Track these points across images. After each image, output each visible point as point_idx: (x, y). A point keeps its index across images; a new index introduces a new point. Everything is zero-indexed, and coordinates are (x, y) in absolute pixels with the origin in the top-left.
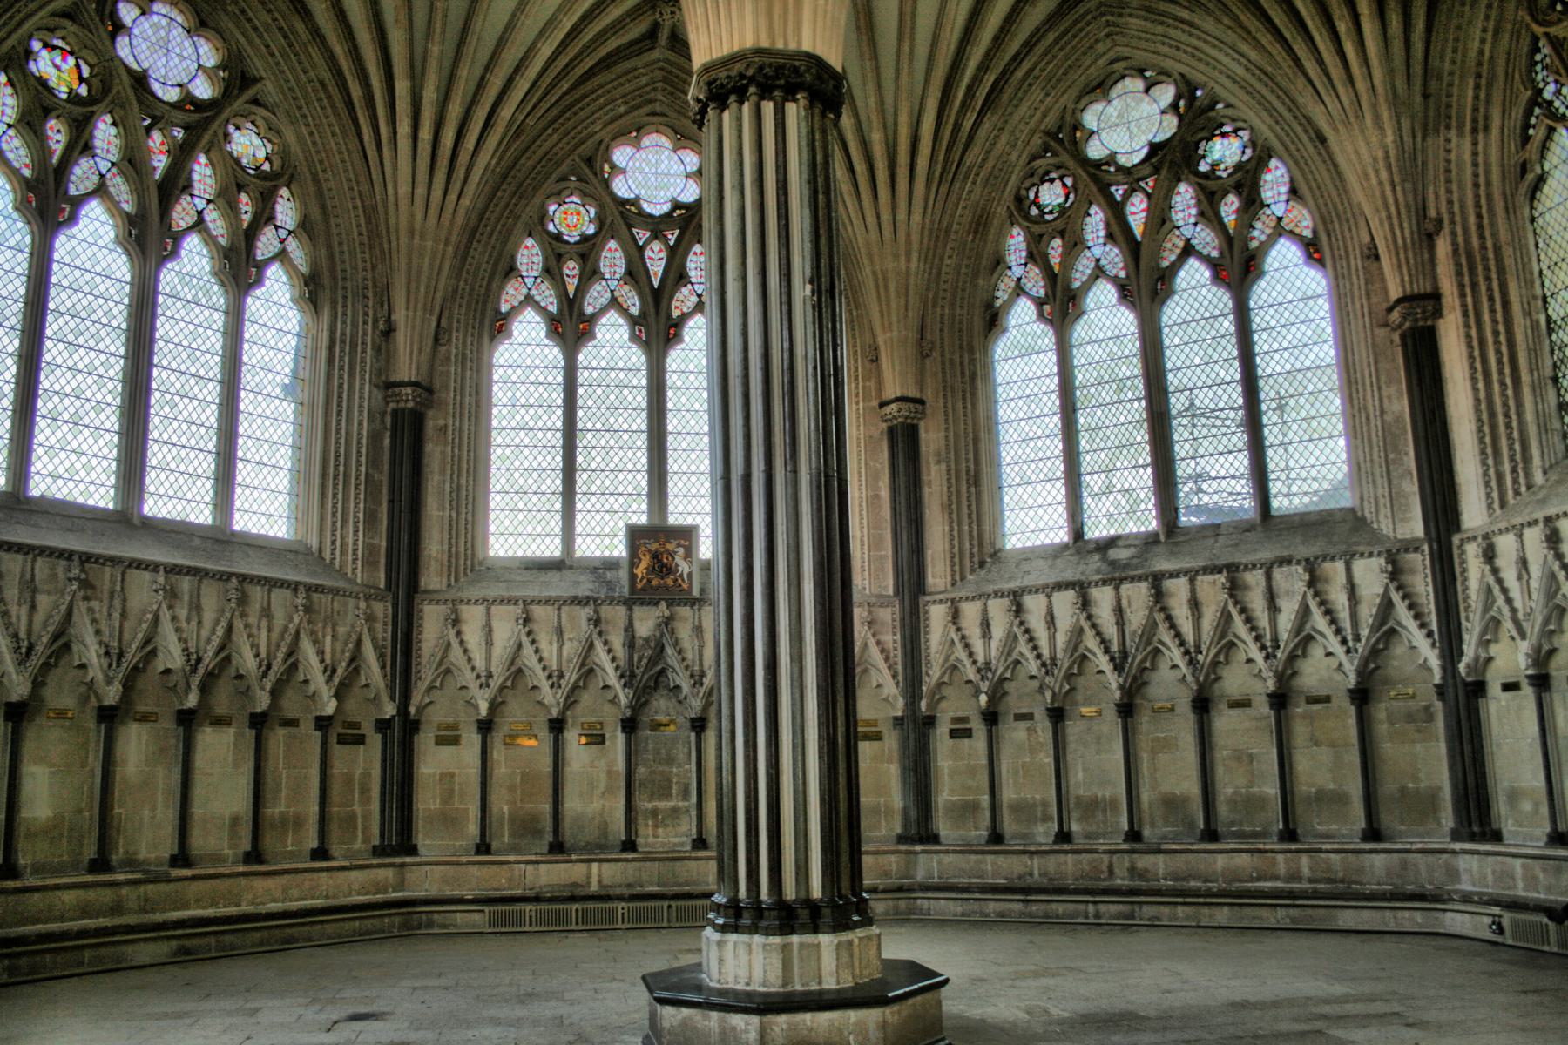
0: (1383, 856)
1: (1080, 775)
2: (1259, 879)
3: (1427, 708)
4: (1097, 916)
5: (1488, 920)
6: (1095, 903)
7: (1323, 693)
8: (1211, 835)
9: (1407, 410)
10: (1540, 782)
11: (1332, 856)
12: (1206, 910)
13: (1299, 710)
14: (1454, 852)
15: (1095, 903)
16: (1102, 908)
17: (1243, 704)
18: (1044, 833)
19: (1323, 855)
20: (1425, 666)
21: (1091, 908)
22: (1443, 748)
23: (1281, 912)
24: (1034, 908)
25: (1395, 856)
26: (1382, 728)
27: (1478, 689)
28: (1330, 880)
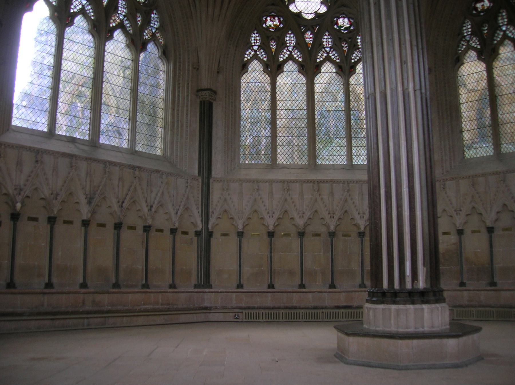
0: (185, 294)
1: (60, 253)
2: (144, 304)
3: (191, 239)
4: (88, 325)
5: (234, 314)
6: (88, 318)
7: (161, 228)
8: (116, 285)
9: (198, 128)
10: (236, 267)
11: (169, 294)
12: (135, 319)
13: (153, 234)
14: (205, 292)
15: (88, 318)
16: (91, 320)
17: (132, 228)
18: (38, 284)
19: (166, 294)
20: (195, 225)
21: (86, 320)
22: (195, 255)
23: (162, 317)
24: (57, 323)
25: (188, 294)
26: (178, 245)
27: (210, 234)
28: (168, 304)
